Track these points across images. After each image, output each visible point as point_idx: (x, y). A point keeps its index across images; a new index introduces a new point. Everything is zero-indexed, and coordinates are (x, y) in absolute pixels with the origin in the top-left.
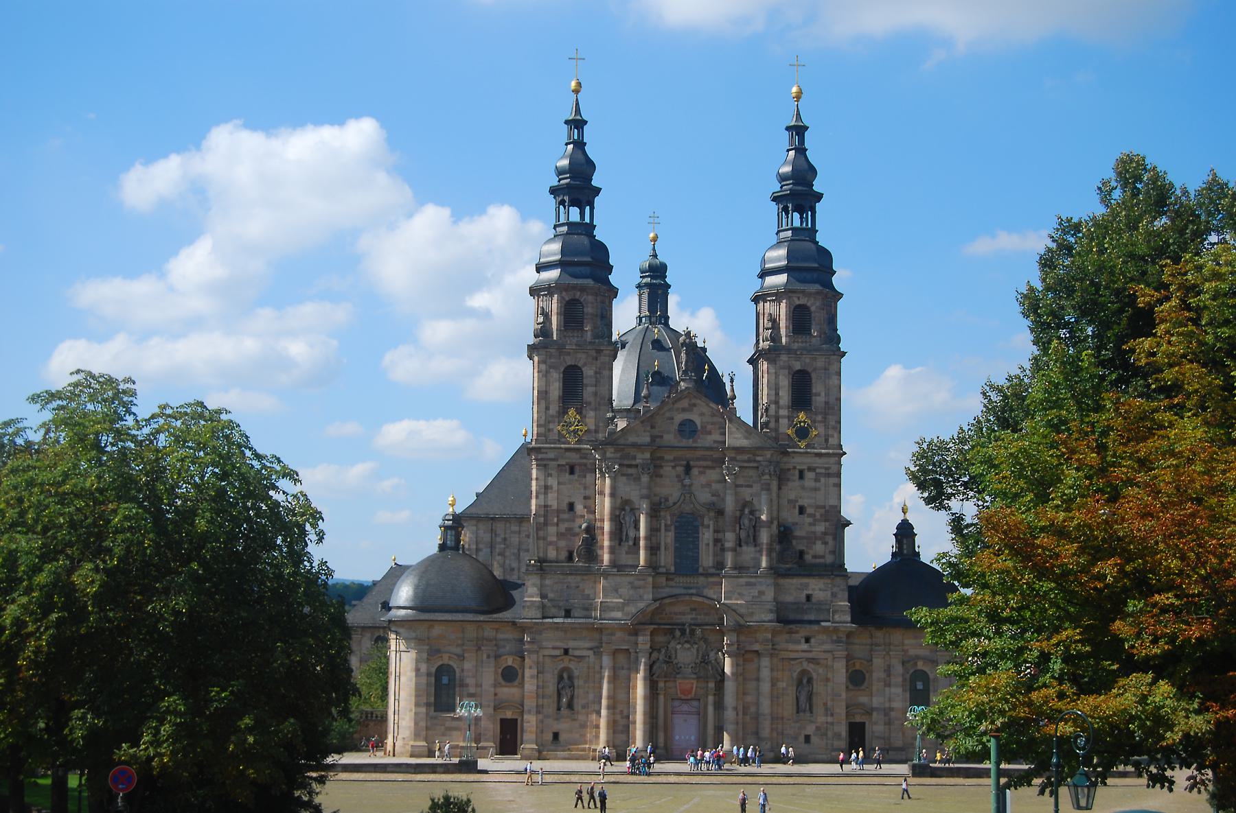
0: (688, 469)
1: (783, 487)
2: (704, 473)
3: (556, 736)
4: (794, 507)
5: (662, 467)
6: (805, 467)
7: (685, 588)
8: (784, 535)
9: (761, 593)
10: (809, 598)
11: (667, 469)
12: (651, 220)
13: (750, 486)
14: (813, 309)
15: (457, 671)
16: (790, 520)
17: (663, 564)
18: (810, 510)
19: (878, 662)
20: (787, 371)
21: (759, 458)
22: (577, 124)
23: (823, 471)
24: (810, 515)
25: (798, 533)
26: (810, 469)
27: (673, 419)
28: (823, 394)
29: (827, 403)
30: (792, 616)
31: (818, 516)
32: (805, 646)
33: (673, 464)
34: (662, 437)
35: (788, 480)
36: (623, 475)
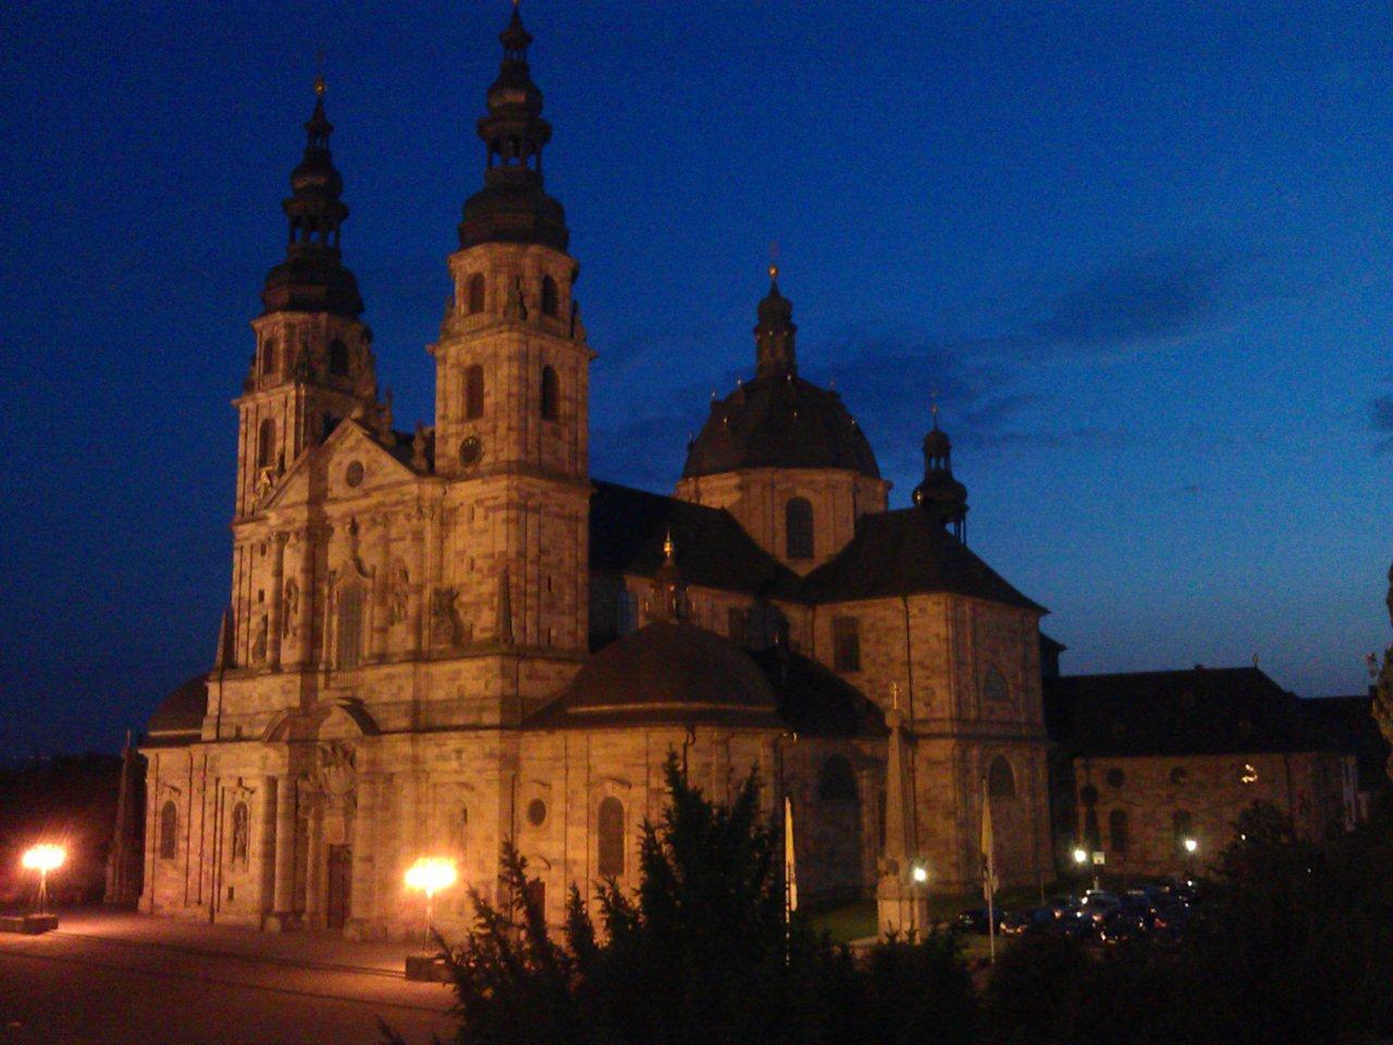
0: (354, 529)
1: (452, 535)
2: (368, 530)
3: (231, 890)
4: (463, 560)
7: (342, 690)
8: (446, 602)
9: (400, 688)
11: (340, 533)
13: (403, 539)
14: (486, 275)
15: (177, 807)
16: (458, 581)
17: (324, 658)
18: (479, 563)
19: (558, 785)
20: (455, 371)
23: (489, 503)
24: (480, 570)
25: (465, 598)
27: (340, 464)
28: (492, 392)
30: (439, 720)
31: (485, 571)
32: (454, 764)
35: (456, 523)
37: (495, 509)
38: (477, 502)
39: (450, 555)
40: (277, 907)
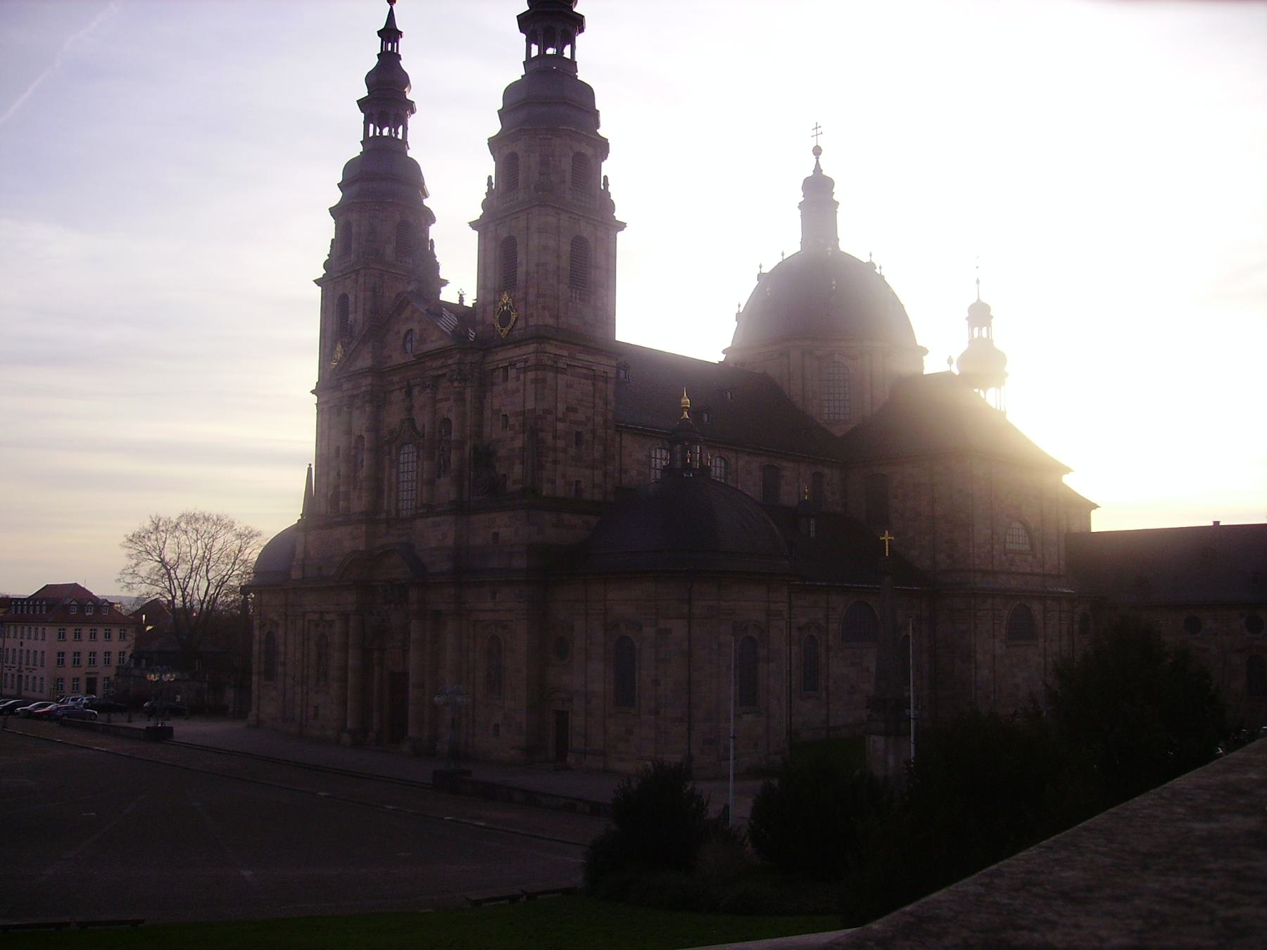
5: (393, 391)
6: (507, 364)
8: (484, 457)
10: (496, 535)
12: (814, 132)
14: (520, 155)
17: (385, 507)
18: (512, 421)
21: (450, 361)
22: (390, 33)
23: (522, 365)
26: (512, 365)
27: (399, 332)
29: (527, 273)
33: (397, 387)
34: (390, 357)
35: (493, 384)
36: (357, 408)
37: (525, 370)
38: (510, 365)
39: (488, 413)
40: (349, 725)
